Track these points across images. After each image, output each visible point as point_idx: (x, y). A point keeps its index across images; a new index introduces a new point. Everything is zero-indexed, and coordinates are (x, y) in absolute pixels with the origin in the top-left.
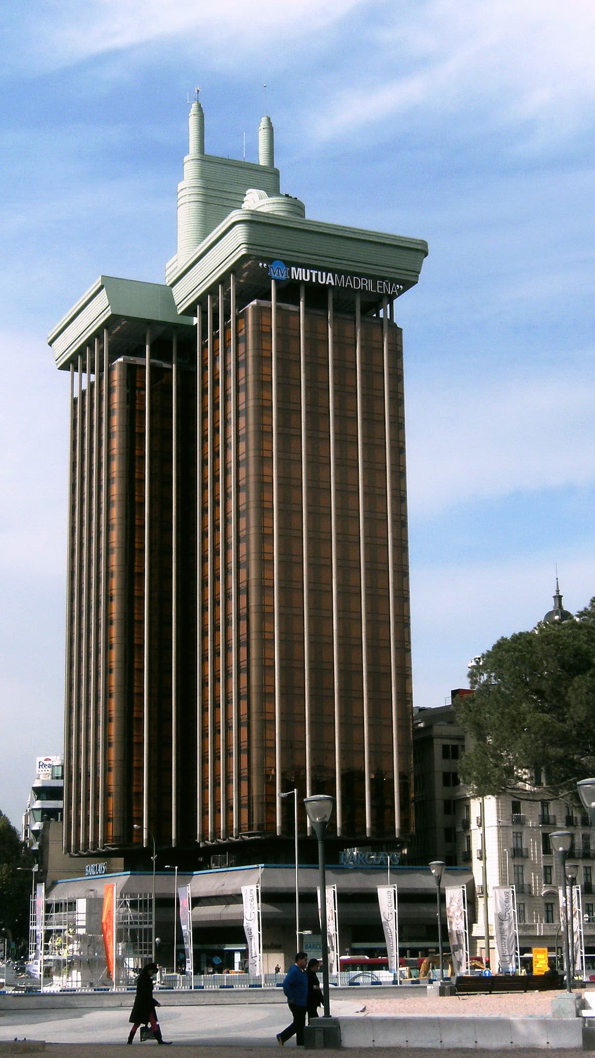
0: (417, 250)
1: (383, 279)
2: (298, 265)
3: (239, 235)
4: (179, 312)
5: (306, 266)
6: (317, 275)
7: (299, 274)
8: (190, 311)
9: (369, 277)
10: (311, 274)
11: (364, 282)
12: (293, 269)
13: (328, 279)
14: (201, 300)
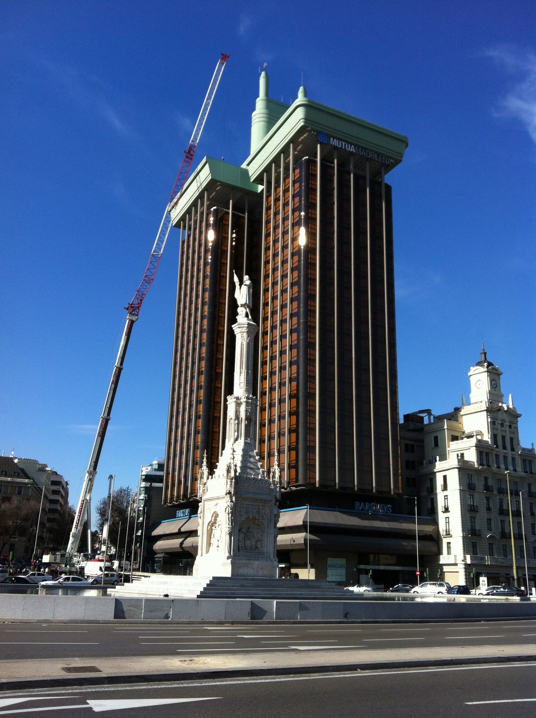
0: (403, 141)
1: (383, 155)
2: (334, 138)
3: (300, 114)
4: (252, 180)
5: (340, 139)
6: (345, 145)
7: (334, 142)
8: (259, 180)
9: (376, 152)
10: (342, 144)
11: (372, 154)
12: (332, 139)
13: (352, 149)
14: (268, 169)
